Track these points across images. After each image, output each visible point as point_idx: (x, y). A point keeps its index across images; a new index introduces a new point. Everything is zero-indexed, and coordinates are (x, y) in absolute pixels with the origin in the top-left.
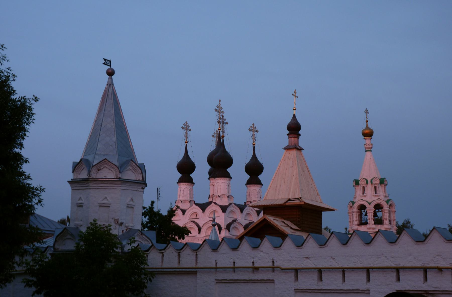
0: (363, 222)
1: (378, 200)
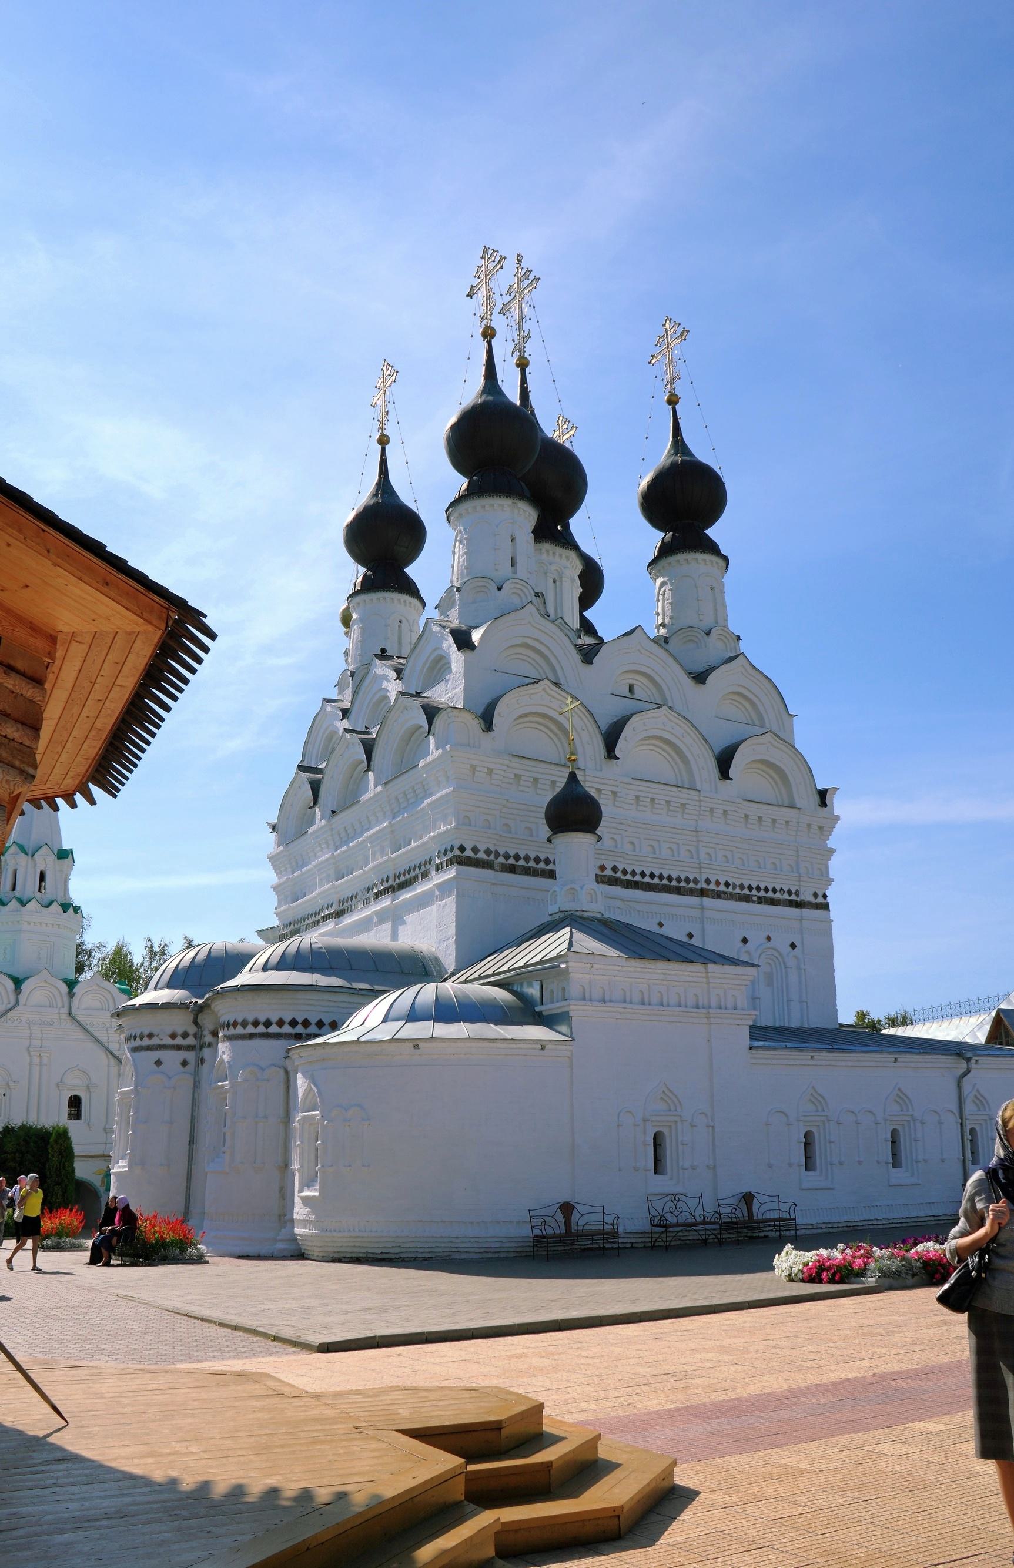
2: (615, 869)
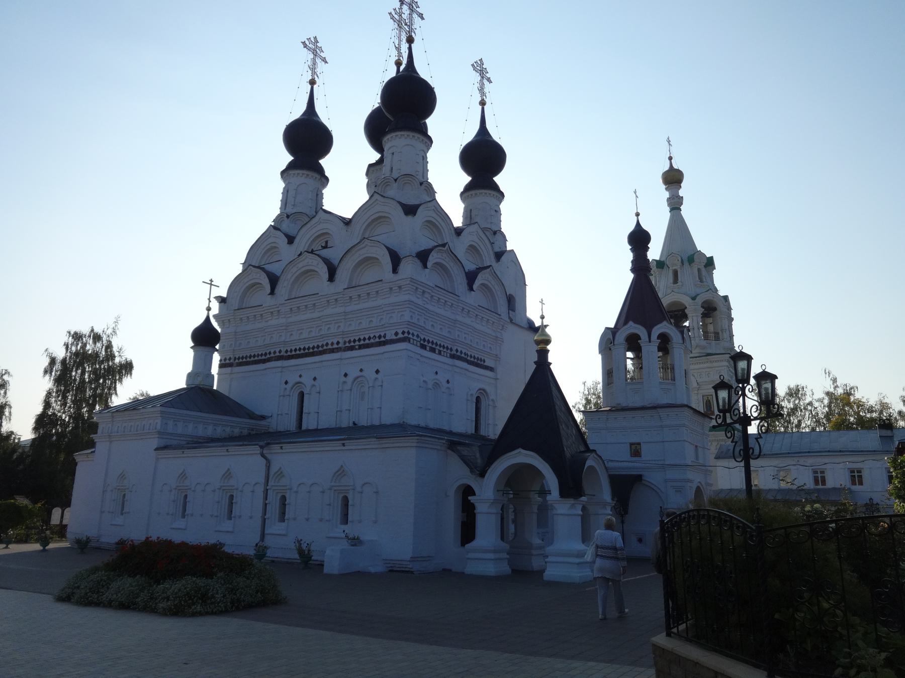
2: (280, 352)
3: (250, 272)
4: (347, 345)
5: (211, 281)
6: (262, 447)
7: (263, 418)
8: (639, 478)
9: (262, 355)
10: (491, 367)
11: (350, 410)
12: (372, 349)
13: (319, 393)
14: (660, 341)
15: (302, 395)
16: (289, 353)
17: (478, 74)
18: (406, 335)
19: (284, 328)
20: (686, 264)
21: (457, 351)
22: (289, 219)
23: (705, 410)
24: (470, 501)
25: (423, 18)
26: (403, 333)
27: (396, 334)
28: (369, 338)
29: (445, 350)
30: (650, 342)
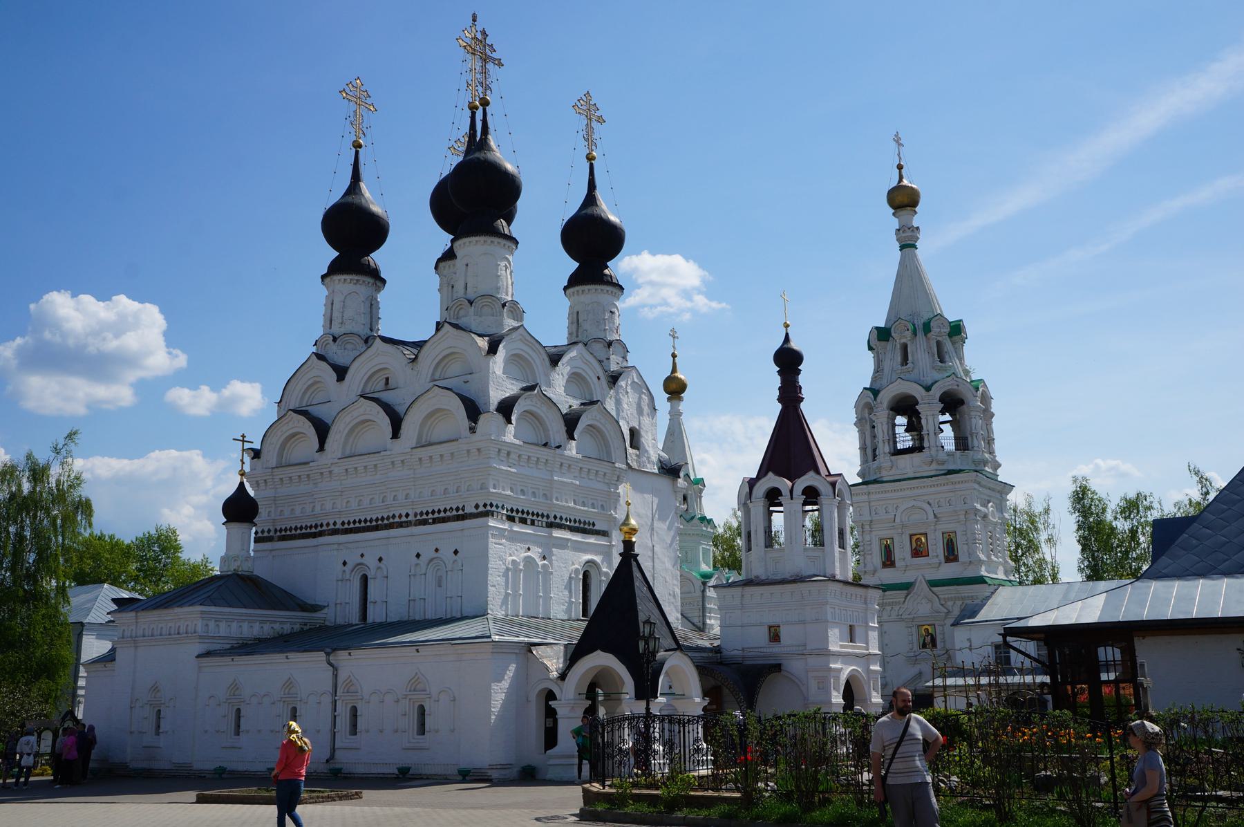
0: (900, 446)
1: (949, 379)
2: (335, 524)
3: (290, 418)
4: (419, 517)
5: (243, 436)
6: (328, 654)
7: (315, 608)
8: (777, 668)
9: (311, 527)
10: (603, 531)
11: (425, 599)
12: (449, 523)
13: (387, 577)
14: (805, 497)
15: (365, 579)
16: (346, 526)
17: (584, 117)
18: (488, 508)
19: (338, 494)
20: (920, 334)
21: (555, 517)
22: (337, 341)
23: (946, 554)
24: (550, 705)
25: (500, 64)
26: (485, 505)
27: (477, 506)
28: (445, 511)
29: (540, 518)
30: (792, 499)
